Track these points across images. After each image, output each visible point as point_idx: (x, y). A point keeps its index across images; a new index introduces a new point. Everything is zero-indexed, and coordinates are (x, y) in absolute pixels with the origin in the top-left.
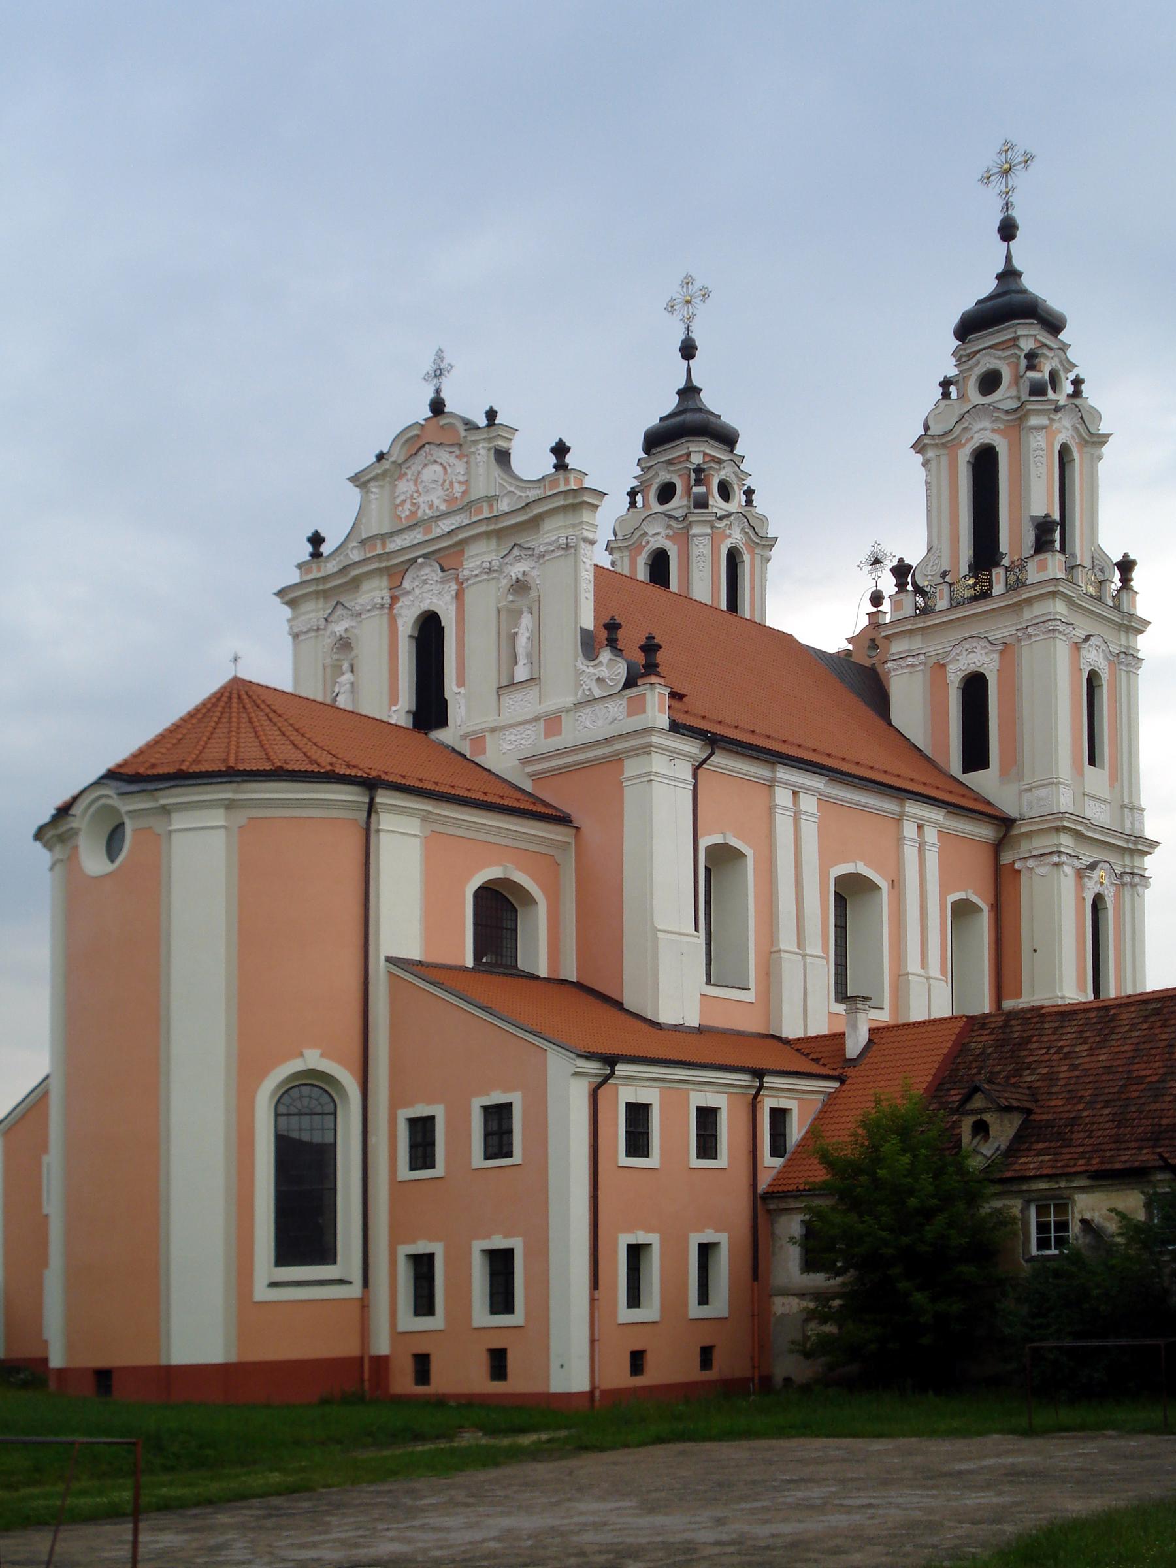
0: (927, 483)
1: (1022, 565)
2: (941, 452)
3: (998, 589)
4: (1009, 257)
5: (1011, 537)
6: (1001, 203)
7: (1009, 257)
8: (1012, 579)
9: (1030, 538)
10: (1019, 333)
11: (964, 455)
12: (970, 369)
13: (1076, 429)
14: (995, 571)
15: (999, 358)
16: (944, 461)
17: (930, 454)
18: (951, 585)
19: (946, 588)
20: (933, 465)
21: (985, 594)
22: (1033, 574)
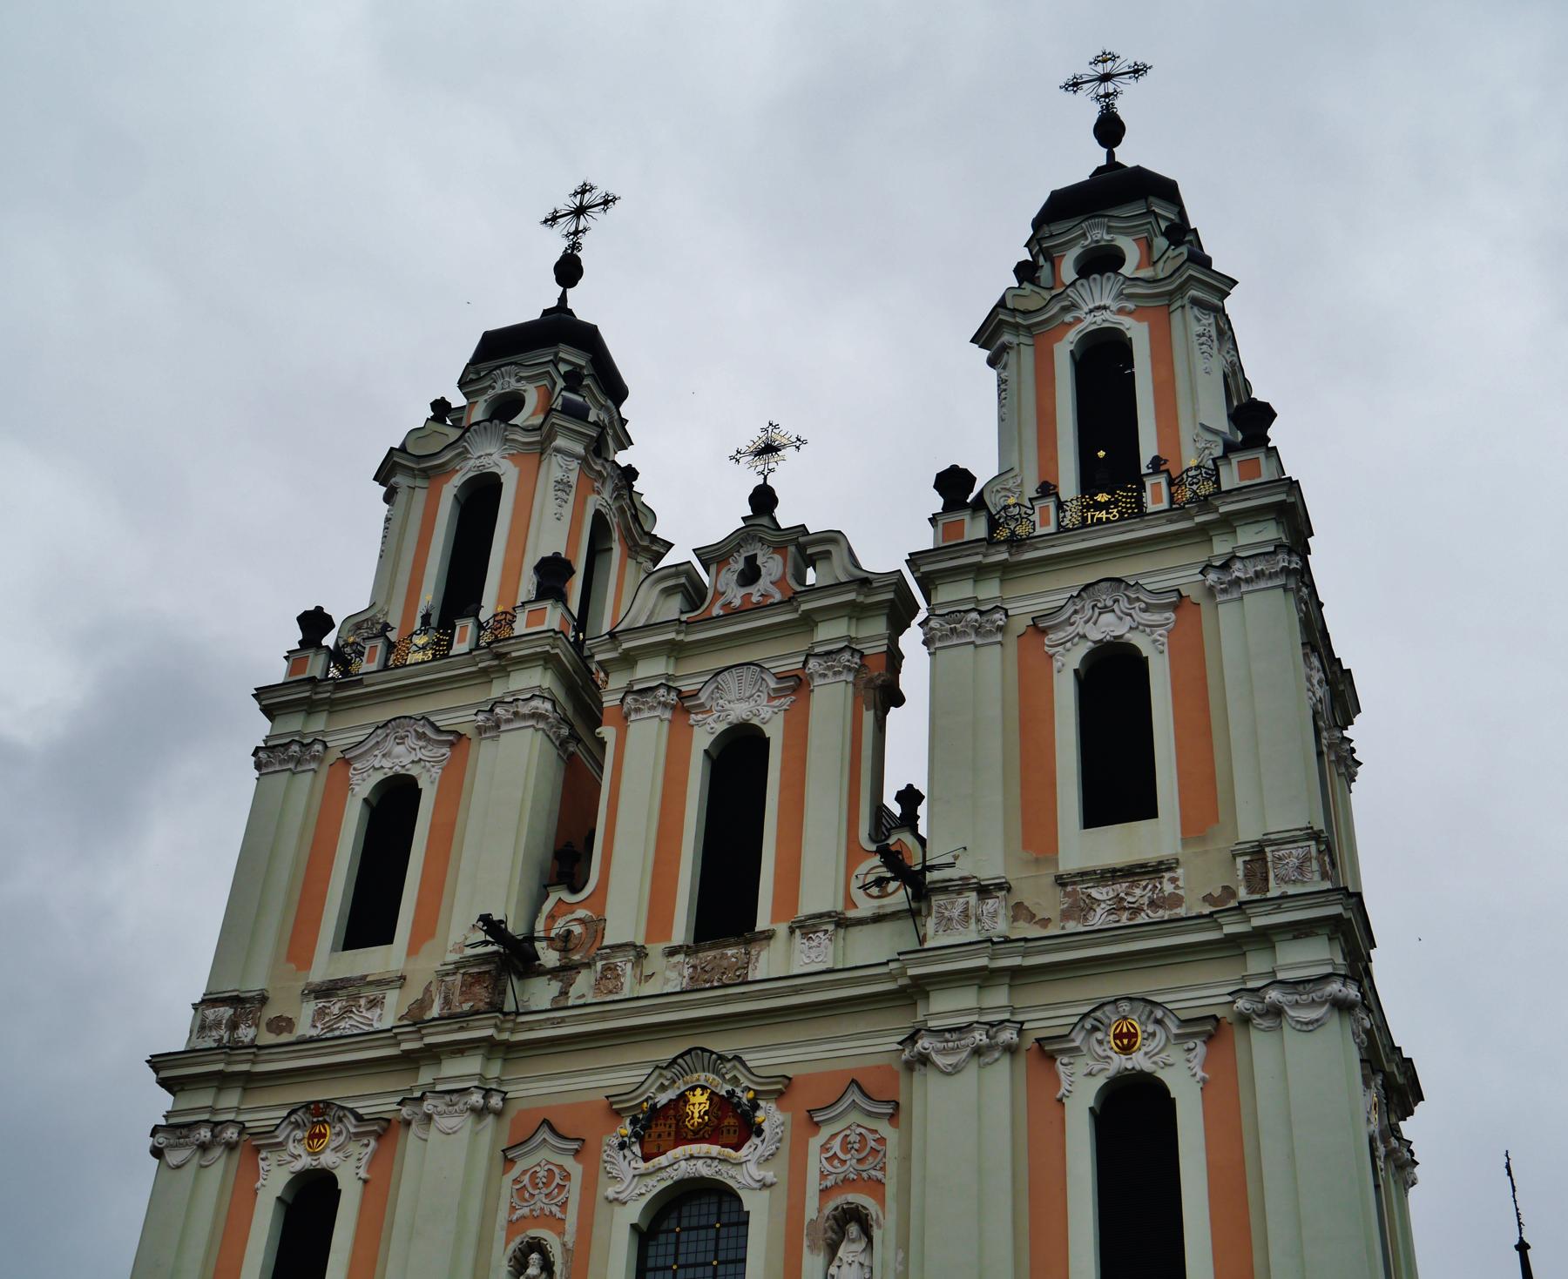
0: (388, 520)
1: (505, 619)
2: (419, 482)
3: (459, 647)
4: (563, 299)
5: (505, 581)
6: (565, 243)
7: (563, 299)
8: (486, 637)
9: (528, 585)
10: (561, 355)
11: (449, 490)
12: (483, 391)
13: (621, 510)
14: (459, 623)
15: (529, 379)
16: (420, 497)
17: (399, 480)
18: (391, 647)
19: (380, 644)
20: (401, 498)
21: (441, 649)
22: (520, 627)
